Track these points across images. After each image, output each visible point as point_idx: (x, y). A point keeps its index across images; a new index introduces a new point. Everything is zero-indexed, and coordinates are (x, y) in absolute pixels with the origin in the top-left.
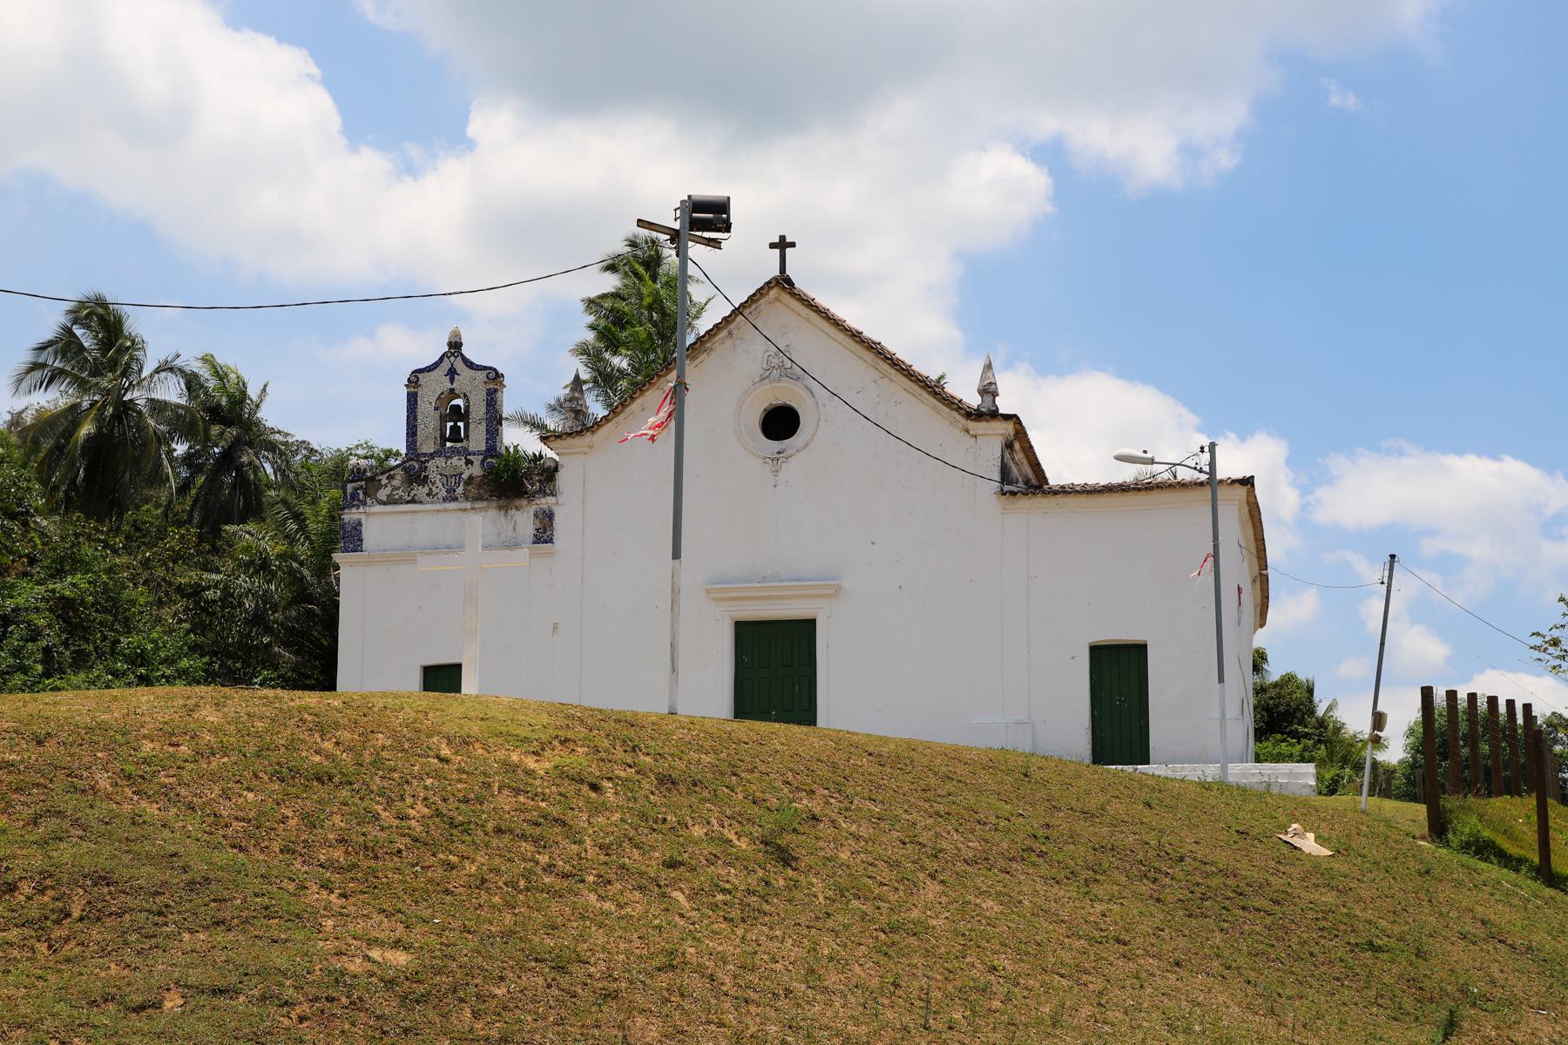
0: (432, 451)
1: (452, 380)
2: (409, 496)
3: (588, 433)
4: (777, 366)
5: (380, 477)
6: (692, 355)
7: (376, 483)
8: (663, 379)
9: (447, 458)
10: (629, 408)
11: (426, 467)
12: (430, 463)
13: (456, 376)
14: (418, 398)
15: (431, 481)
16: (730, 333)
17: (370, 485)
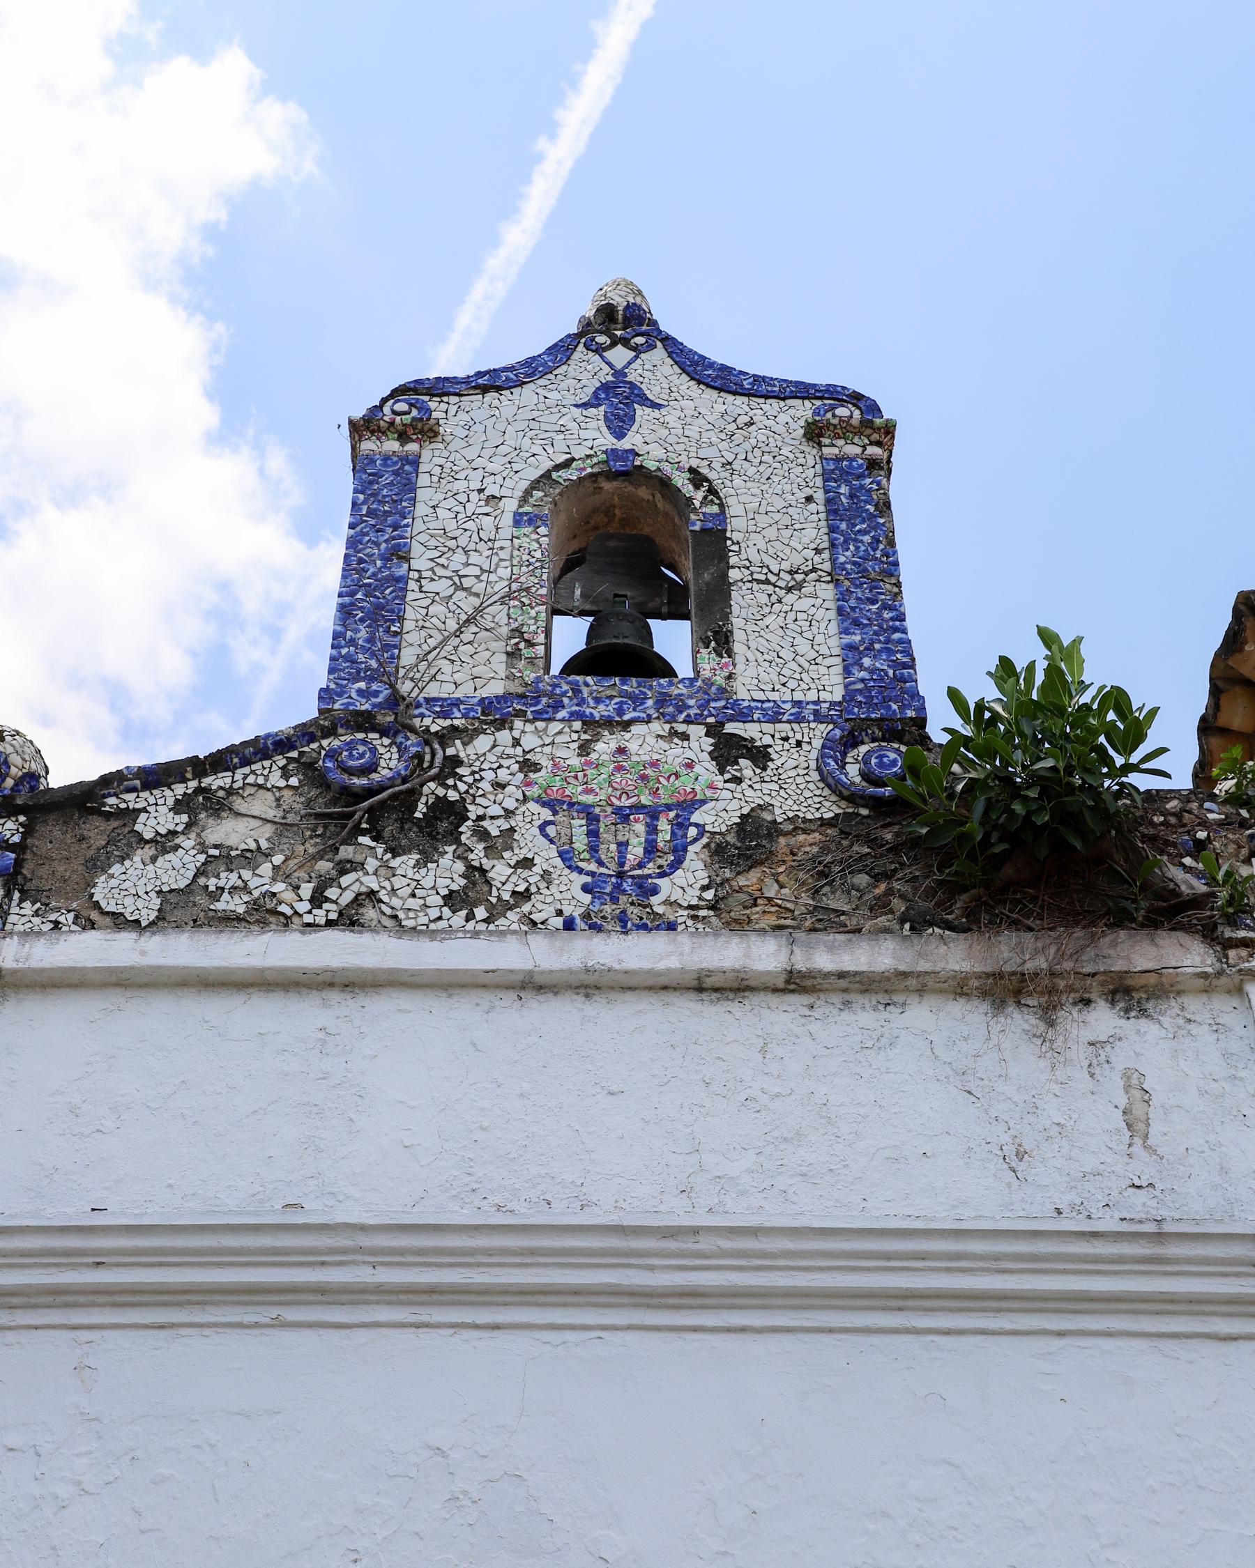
0: (496, 688)
1: (619, 424)
2: (318, 900)
5: (131, 800)
7: (96, 831)
9: (590, 724)
11: (456, 761)
12: (482, 743)
13: (641, 412)
14: (423, 480)
15: (483, 835)
17: (52, 837)
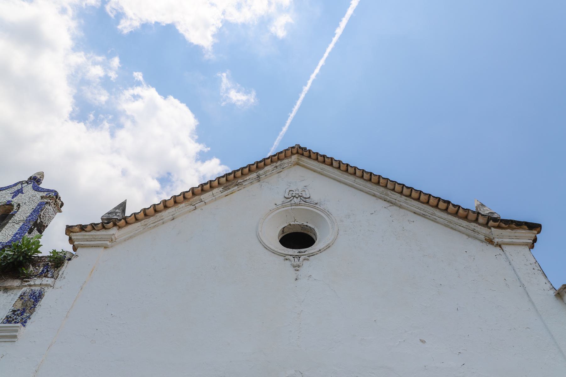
3: (115, 228)
4: (297, 196)
6: (225, 185)
8: (197, 197)
10: (160, 214)
16: (258, 177)
